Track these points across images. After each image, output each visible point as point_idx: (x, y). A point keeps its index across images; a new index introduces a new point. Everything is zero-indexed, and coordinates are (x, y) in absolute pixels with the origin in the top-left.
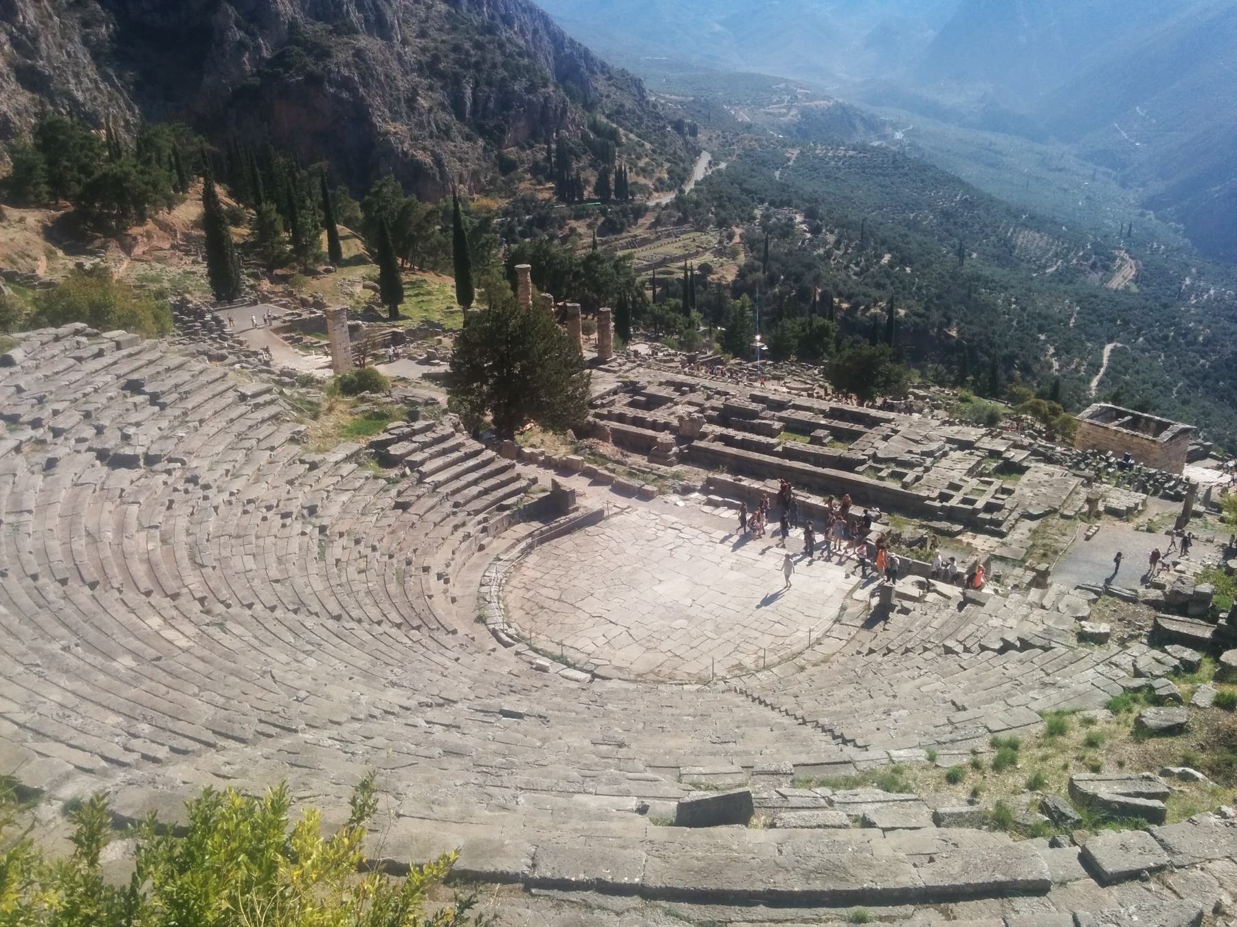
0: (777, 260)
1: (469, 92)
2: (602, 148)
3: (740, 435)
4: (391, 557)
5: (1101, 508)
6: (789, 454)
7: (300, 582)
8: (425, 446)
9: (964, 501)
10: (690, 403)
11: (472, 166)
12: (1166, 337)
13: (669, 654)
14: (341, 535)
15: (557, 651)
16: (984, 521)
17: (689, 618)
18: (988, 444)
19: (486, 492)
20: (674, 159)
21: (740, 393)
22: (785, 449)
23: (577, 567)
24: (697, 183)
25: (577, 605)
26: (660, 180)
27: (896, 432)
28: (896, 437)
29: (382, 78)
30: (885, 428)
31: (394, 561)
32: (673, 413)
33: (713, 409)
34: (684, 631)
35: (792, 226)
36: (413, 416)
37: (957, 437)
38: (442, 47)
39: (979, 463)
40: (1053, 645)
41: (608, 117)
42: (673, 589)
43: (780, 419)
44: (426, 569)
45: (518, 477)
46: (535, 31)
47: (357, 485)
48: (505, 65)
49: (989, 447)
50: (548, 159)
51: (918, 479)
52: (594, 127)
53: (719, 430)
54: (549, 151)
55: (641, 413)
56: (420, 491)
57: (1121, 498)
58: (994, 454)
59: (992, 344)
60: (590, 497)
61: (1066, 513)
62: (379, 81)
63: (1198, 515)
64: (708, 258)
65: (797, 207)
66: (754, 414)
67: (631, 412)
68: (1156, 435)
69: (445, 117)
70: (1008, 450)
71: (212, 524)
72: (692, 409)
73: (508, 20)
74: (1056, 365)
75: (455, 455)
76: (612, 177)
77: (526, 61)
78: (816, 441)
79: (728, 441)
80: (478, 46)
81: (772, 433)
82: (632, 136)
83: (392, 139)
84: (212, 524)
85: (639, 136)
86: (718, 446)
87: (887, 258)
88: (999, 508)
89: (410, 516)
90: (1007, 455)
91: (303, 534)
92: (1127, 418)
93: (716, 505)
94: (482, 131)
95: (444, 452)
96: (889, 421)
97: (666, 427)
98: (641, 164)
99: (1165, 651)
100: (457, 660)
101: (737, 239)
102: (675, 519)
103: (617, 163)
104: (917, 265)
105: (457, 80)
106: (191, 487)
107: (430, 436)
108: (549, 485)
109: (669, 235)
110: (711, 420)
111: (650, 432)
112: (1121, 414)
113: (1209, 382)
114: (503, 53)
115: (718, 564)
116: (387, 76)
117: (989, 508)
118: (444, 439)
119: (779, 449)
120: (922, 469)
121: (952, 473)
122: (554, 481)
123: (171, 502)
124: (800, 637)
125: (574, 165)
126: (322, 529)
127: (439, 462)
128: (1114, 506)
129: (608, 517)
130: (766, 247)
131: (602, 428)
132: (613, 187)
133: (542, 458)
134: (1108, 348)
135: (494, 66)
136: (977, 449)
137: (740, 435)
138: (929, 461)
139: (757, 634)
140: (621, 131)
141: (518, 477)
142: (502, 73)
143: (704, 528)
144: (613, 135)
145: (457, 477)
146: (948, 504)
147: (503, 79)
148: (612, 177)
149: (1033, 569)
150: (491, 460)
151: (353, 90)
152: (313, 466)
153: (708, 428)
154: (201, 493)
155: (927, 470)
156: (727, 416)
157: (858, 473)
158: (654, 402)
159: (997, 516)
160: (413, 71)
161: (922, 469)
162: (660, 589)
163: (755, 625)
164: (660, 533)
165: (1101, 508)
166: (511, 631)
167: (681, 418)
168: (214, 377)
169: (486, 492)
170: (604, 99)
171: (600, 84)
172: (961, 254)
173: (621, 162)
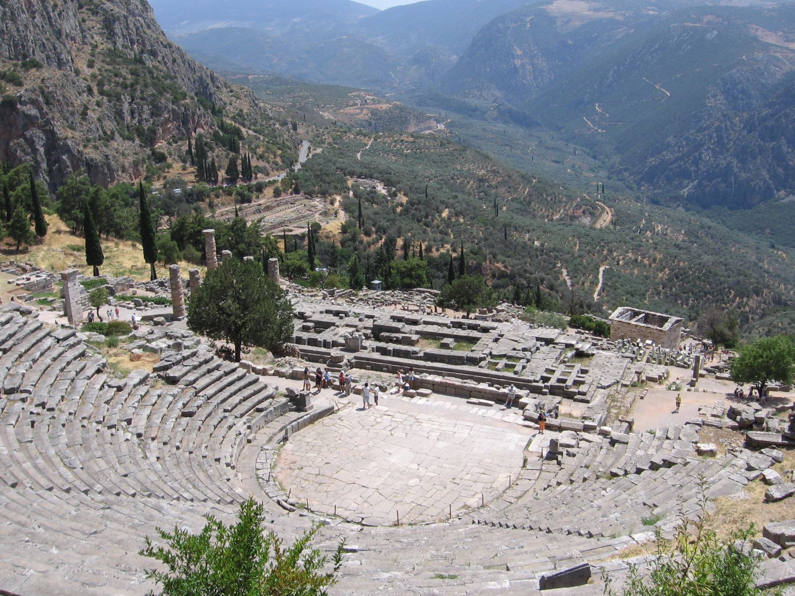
1: (126, 107)
2: (230, 139)
3: (391, 346)
4: (191, 453)
5: (644, 378)
6: (429, 357)
7: (140, 476)
8: (195, 368)
10: (347, 326)
11: (131, 159)
12: (636, 260)
13: (414, 505)
14: (153, 439)
15: (332, 512)
16: (575, 394)
17: (418, 477)
18: (562, 340)
20: (283, 147)
21: (384, 315)
23: (325, 449)
24: (303, 165)
25: (335, 476)
26: (276, 164)
27: (502, 336)
28: (502, 340)
29: (61, 98)
30: (494, 334)
31: (193, 455)
32: (336, 334)
33: (365, 328)
34: (419, 487)
35: (375, 193)
36: (178, 347)
38: (105, 74)
39: (561, 354)
40: (688, 460)
41: (233, 118)
42: (400, 458)
43: (417, 333)
44: (218, 460)
45: (266, 387)
46: (174, 61)
47: (154, 401)
48: (155, 85)
49: (565, 341)
50: (189, 152)
51: (524, 367)
52: (222, 126)
54: (190, 145)
55: (313, 335)
57: (655, 371)
58: (569, 346)
59: (525, 271)
61: (624, 383)
62: (59, 101)
63: (702, 376)
64: (317, 218)
65: (377, 179)
66: (397, 330)
67: (305, 335)
68: (661, 326)
69: (110, 125)
70: (578, 343)
71: (64, 439)
72: (351, 330)
73: (153, 54)
74: (569, 283)
75: (216, 374)
78: (445, 346)
80: (134, 73)
81: (412, 343)
82: (250, 132)
83: (69, 142)
84: (64, 439)
85: (255, 131)
86: (377, 356)
87: (445, 214)
88: (583, 383)
89: (197, 421)
90: (577, 346)
91: (127, 440)
92: (641, 316)
93: (412, 396)
94: (140, 132)
95: (209, 371)
96: (494, 329)
97: (335, 344)
98: (260, 151)
99: (762, 453)
100: (273, 522)
101: (337, 204)
102: (386, 409)
103: (241, 152)
104: (468, 218)
106: (40, 410)
109: (287, 203)
110: (367, 337)
111: (323, 349)
112: (637, 314)
114: (153, 77)
115: (428, 438)
116: (64, 97)
117: (577, 383)
119: (421, 354)
120: (525, 361)
123: (33, 423)
124: (502, 479)
125: (209, 154)
126: (139, 435)
128: (650, 376)
130: (360, 208)
131: (293, 350)
132: (240, 168)
133: (272, 372)
134: (602, 269)
135: (146, 86)
136: (557, 344)
137: (391, 346)
138: (528, 354)
139: (472, 483)
140: (243, 130)
141: (266, 387)
142: (151, 91)
143: (410, 413)
144: (238, 132)
145: (221, 390)
146: (548, 384)
147: (153, 95)
149: (626, 422)
150: (244, 376)
151: (40, 109)
152: (120, 389)
153: (367, 343)
154: (50, 414)
155: (528, 361)
156: (377, 332)
157: (480, 367)
158: (321, 326)
159: (583, 388)
160: (84, 92)
161: (525, 361)
162: (392, 459)
163: (468, 477)
164: (379, 420)
165: (644, 378)
166: (291, 500)
167: (346, 338)
169: (245, 399)
170: (228, 107)
171: (223, 96)
172: (496, 207)
173: (244, 151)
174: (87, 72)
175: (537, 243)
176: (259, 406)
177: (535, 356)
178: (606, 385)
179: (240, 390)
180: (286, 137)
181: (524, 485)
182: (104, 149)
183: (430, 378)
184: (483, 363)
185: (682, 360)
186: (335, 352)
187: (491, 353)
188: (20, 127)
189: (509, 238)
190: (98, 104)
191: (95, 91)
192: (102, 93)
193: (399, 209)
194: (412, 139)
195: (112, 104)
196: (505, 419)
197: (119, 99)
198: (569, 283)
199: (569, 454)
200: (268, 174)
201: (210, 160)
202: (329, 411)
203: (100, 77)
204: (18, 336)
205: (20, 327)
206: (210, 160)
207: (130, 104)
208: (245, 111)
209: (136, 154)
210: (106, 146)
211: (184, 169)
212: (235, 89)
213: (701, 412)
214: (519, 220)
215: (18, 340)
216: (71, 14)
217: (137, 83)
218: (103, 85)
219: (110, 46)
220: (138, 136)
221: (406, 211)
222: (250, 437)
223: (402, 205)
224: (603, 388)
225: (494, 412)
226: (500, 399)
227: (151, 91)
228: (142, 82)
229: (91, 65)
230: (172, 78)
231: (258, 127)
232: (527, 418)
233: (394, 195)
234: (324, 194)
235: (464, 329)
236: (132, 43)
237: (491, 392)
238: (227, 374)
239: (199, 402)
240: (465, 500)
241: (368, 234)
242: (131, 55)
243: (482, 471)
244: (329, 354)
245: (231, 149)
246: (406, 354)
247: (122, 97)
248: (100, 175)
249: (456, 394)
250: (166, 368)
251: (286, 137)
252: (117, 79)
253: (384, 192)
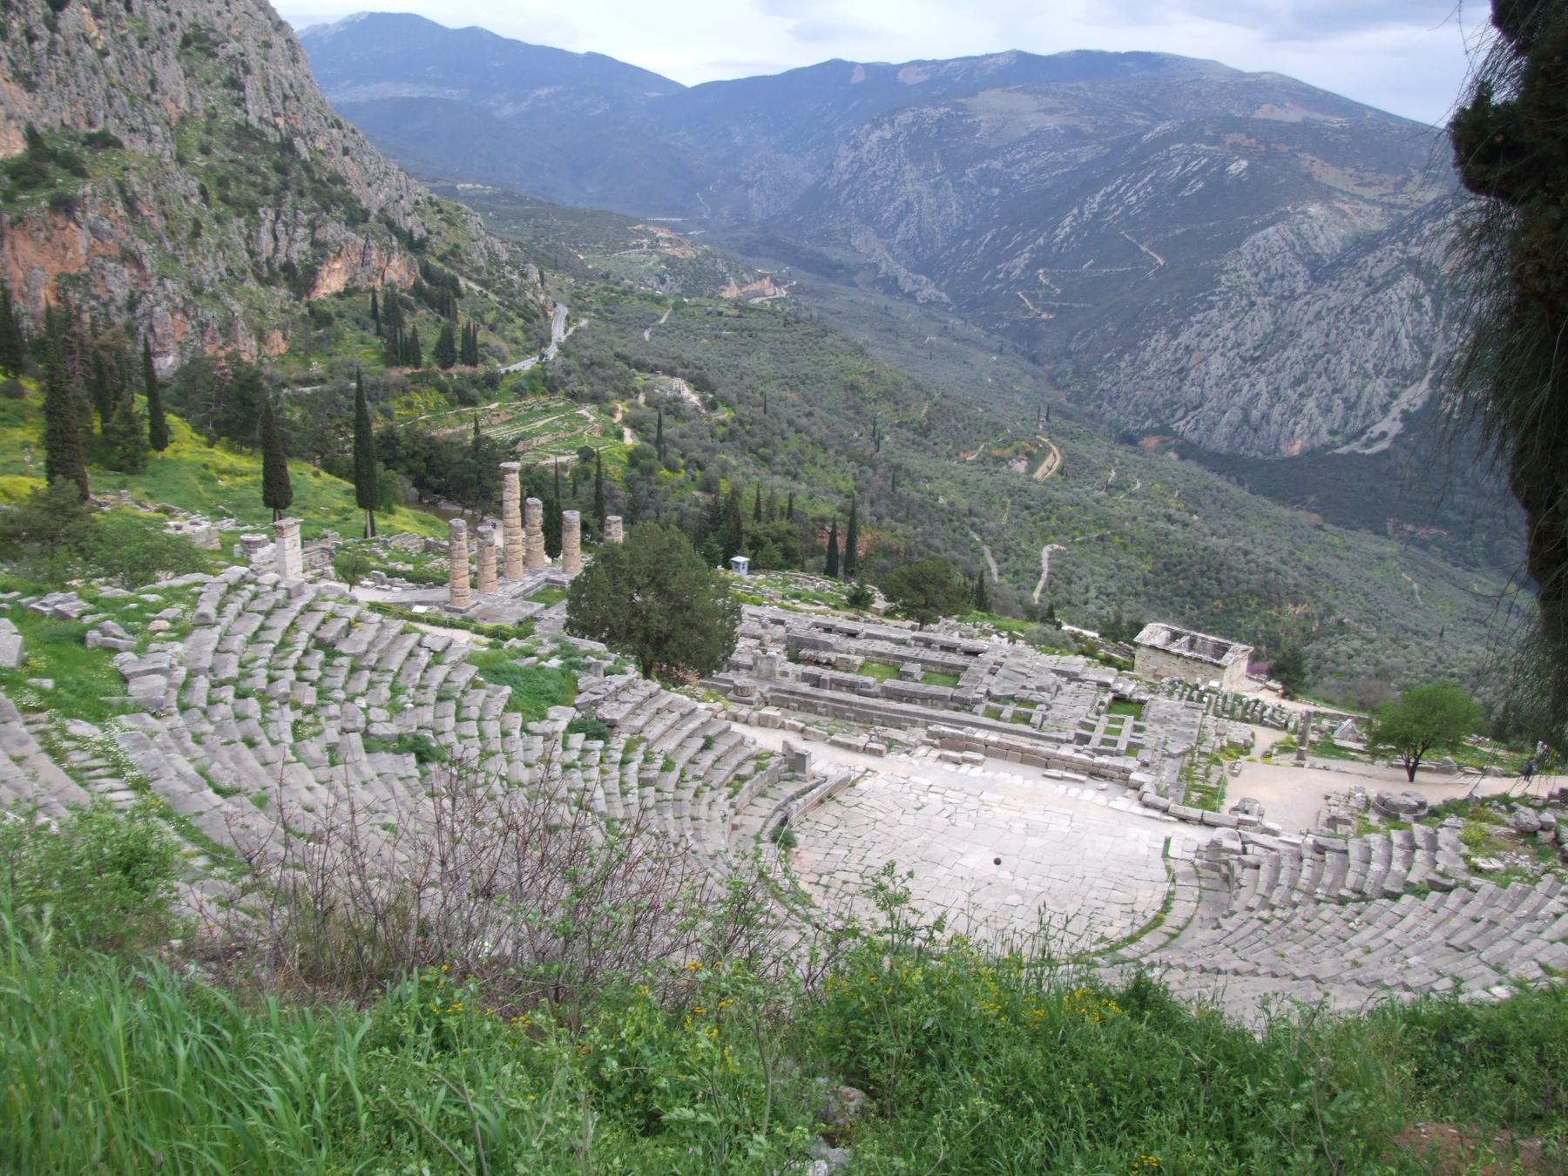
0: (675, 444)
1: (268, 224)
3: (827, 674)
9: (1104, 742)
22: (885, 689)
27: (1001, 664)
28: (1001, 671)
35: (681, 400)
37: (1059, 667)
41: (441, 259)
48: (317, 194)
50: (374, 314)
51: (1044, 718)
52: (427, 272)
53: (800, 668)
59: (930, 546)
60: (825, 761)
61: (1202, 749)
65: (683, 376)
66: (828, 647)
68: (1219, 657)
73: (310, 136)
74: (994, 569)
76: (458, 335)
77: (338, 188)
79: (817, 682)
80: (281, 170)
82: (471, 284)
85: (476, 281)
86: (805, 688)
87: (795, 442)
88: (1141, 746)
90: (1120, 686)
92: (1185, 639)
98: (490, 317)
101: (619, 416)
104: (831, 452)
105: (253, 208)
108: (779, 748)
113: (1150, 589)
114: (312, 179)
121: (1076, 710)
122: (785, 743)
125: (407, 319)
132: (458, 347)
134: (1046, 552)
135: (301, 194)
137: (827, 674)
138: (1047, 696)
140: (462, 282)
147: (313, 210)
148: (458, 335)
153: (790, 667)
155: (1049, 708)
156: (796, 649)
161: (1043, 707)
163: (1093, 894)
164: (924, 800)
170: (434, 239)
173: (463, 319)
174: (200, 161)
175: (941, 500)
177: (1058, 700)
178: (1176, 751)
180: (529, 295)
181: (1180, 910)
182: (229, 300)
183: (980, 735)
184: (980, 708)
185: (1272, 717)
187: (988, 693)
188: (82, 251)
189: (899, 489)
190: (218, 219)
191: (213, 195)
192: (225, 200)
193: (721, 430)
194: (735, 312)
195: (242, 221)
196: (1113, 804)
197: (255, 212)
198: (994, 569)
199: (1244, 865)
200: (503, 360)
201: (408, 331)
203: (222, 173)
206: (408, 331)
207: (275, 223)
208: (463, 244)
209: (283, 311)
210: (231, 293)
212: (446, 208)
213: (1331, 801)
214: (915, 461)
215: (381, 651)
216: (171, 54)
217: (286, 187)
218: (228, 187)
219: (239, 115)
220: (286, 279)
221: (732, 435)
223: (724, 424)
224: (1171, 756)
225: (1090, 795)
226: (1095, 773)
227: (308, 202)
228: (294, 187)
229: (205, 150)
230: (343, 183)
231: (485, 276)
232: (1147, 805)
233: (712, 406)
234: (595, 398)
235: (934, 650)
236: (276, 115)
237: (1081, 762)
240: (1101, 929)
241: (672, 468)
242: (273, 137)
243: (1111, 885)
244: (731, 682)
245: (442, 313)
246: (852, 687)
247: (261, 210)
249: (1024, 761)
250: (596, 703)
251: (529, 295)
252: (253, 178)
253: (695, 399)
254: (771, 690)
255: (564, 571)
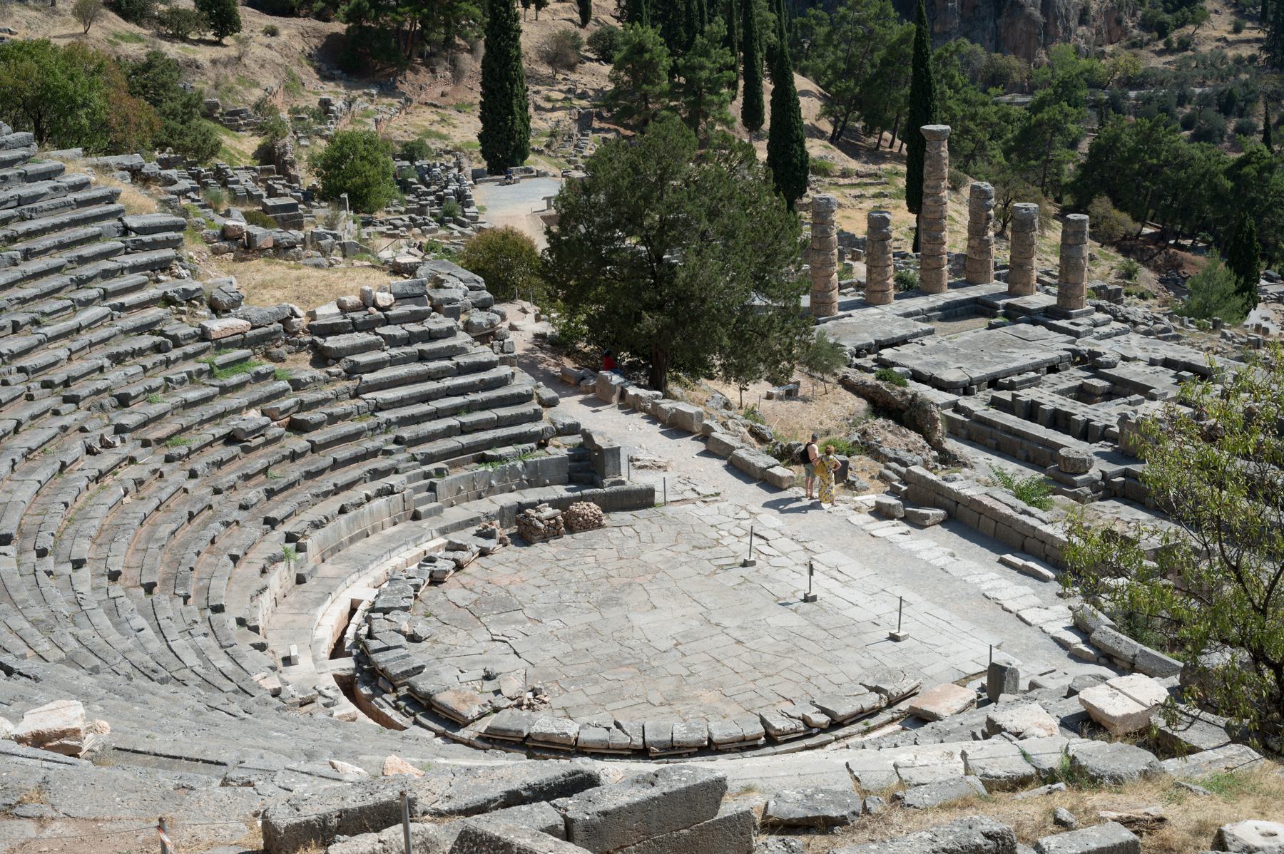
19: (464, 430)
44: (271, 523)
45: (536, 417)
55: (1068, 405)
56: (347, 405)
89: (299, 443)
95: (422, 357)
107: (415, 328)
118: (431, 336)
127: (402, 371)
129: (661, 505)
145: (425, 398)
158: (1120, 388)
168: (98, 193)
169: (464, 430)
176: (488, 452)
179: (470, 408)
186: (1071, 446)
202: (642, 500)
204: (36, 205)
205: (56, 189)
211: (1237, 30)
222: (422, 509)
238: (461, 370)
239: (347, 405)
248: (1021, 25)
250: (333, 330)
254: (1125, 474)
255: (1010, 294)
